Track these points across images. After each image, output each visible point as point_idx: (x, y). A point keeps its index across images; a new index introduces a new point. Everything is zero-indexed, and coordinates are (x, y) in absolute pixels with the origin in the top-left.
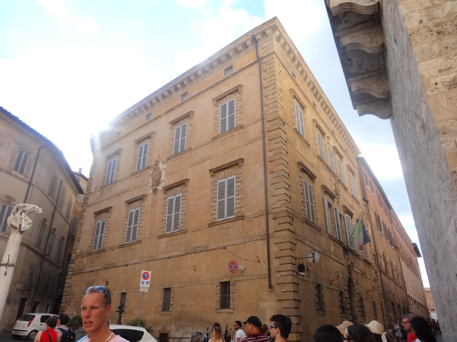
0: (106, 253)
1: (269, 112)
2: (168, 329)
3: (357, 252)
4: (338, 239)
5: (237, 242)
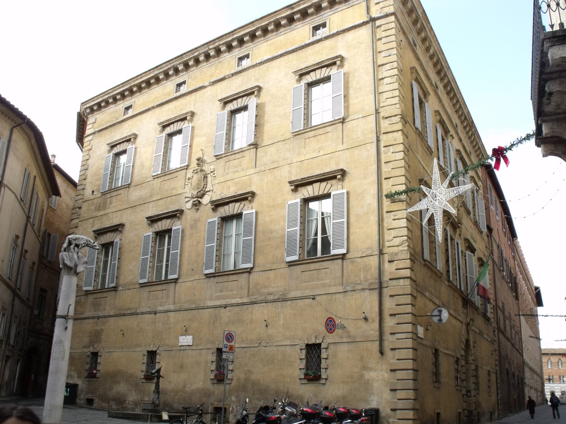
0: (118, 292)
1: (385, 104)
3: (476, 304)
4: (458, 287)
5: (333, 290)
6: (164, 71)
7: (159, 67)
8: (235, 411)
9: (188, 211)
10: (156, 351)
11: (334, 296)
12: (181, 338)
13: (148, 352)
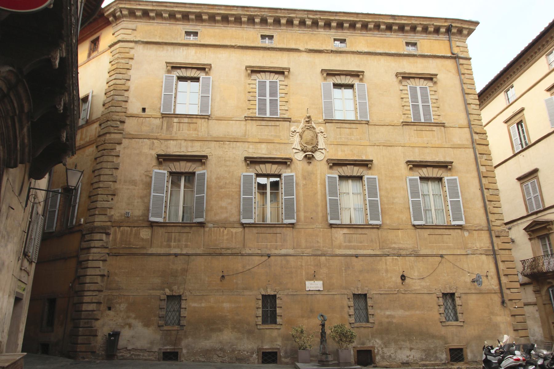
0: (207, 229)
2: (368, 345)
6: (251, 15)
7: (246, 9)
8: (380, 352)
9: (298, 162)
10: (275, 296)
11: (459, 257)
12: (308, 283)
13: (263, 295)
